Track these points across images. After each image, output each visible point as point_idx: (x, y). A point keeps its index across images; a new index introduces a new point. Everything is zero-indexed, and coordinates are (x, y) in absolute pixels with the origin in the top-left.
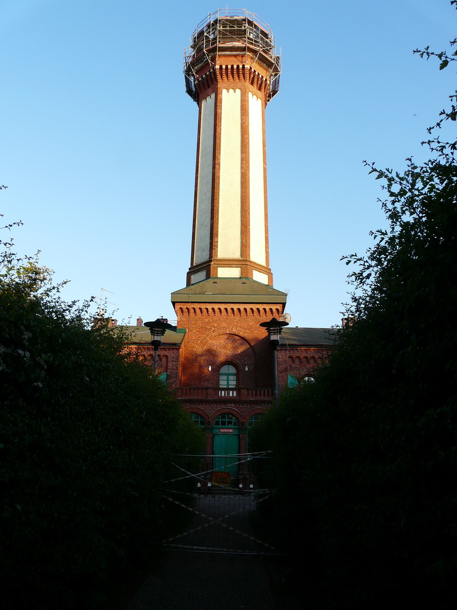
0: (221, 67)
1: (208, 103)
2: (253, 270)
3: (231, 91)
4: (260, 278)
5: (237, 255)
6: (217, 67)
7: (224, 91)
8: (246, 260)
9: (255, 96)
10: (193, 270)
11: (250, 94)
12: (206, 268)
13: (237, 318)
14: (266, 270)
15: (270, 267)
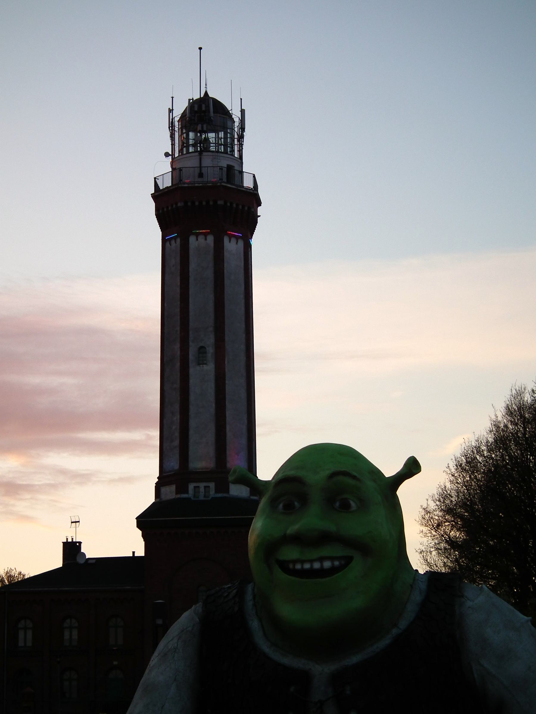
3: (201, 238)
7: (192, 239)
9: (233, 240)
11: (226, 239)
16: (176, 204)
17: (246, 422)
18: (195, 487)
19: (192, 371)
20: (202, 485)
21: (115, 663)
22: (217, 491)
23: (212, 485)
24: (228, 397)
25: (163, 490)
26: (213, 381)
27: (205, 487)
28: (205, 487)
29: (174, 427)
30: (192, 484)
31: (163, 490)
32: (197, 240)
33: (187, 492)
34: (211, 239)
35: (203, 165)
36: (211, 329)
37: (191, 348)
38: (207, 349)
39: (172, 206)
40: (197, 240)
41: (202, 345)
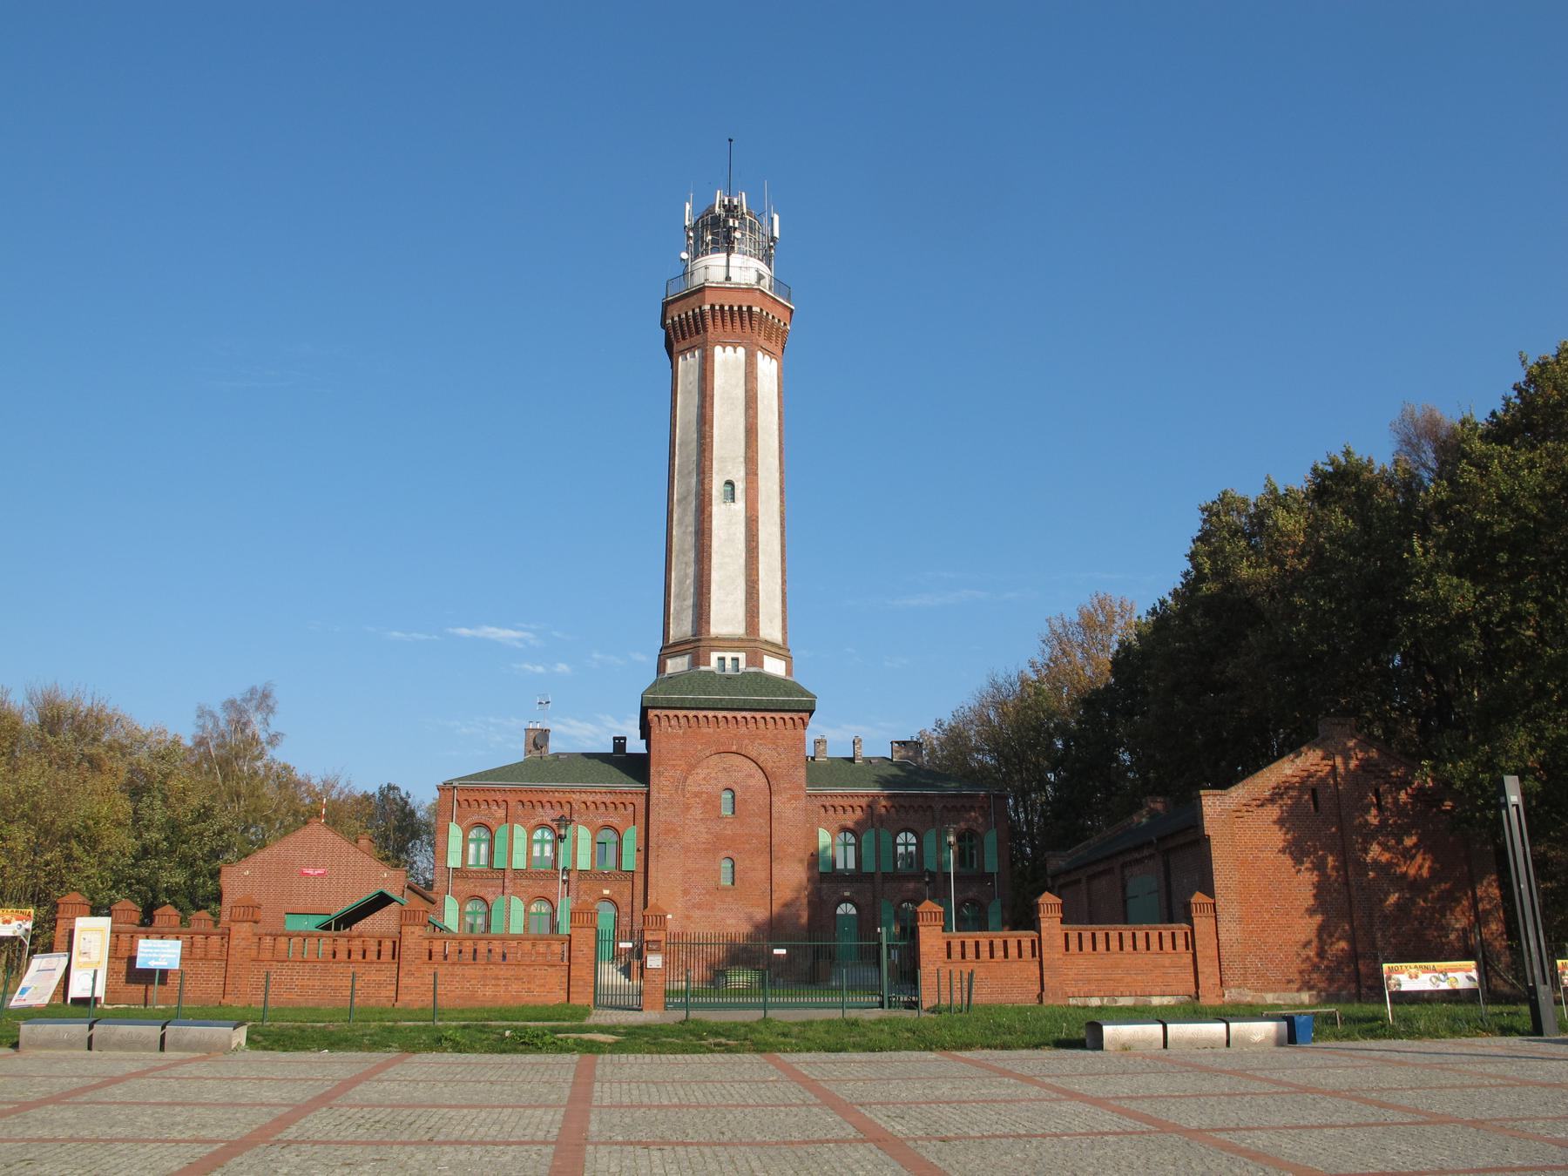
0: (713, 306)
1: (688, 365)
2: (765, 657)
3: (729, 349)
4: (774, 667)
5: (738, 629)
6: (707, 307)
7: (718, 349)
8: (756, 640)
9: (767, 356)
10: (669, 649)
11: (760, 354)
12: (690, 651)
13: (743, 730)
14: (780, 651)
15: (789, 646)
16: (700, 308)
17: (780, 581)
18: (719, 659)
19: (715, 509)
20: (729, 656)
21: (606, 892)
22: (747, 666)
23: (742, 656)
24: (761, 547)
25: (669, 662)
26: (744, 524)
27: (733, 659)
28: (733, 659)
29: (688, 582)
30: (715, 653)
31: (669, 662)
32: (724, 351)
33: (709, 665)
34: (741, 350)
35: (731, 264)
36: (742, 459)
37: (714, 481)
38: (736, 484)
39: (693, 311)
40: (724, 351)
41: (729, 478)
